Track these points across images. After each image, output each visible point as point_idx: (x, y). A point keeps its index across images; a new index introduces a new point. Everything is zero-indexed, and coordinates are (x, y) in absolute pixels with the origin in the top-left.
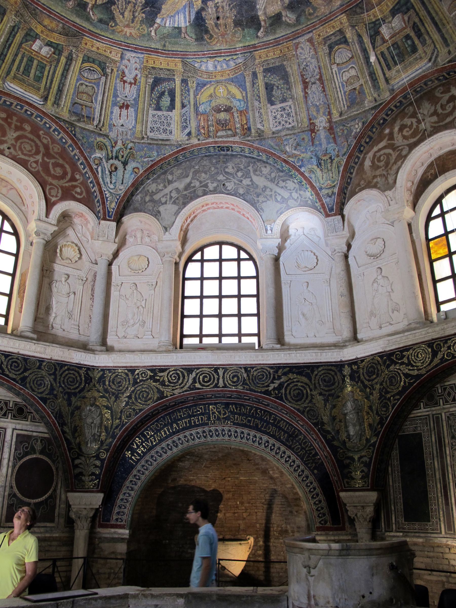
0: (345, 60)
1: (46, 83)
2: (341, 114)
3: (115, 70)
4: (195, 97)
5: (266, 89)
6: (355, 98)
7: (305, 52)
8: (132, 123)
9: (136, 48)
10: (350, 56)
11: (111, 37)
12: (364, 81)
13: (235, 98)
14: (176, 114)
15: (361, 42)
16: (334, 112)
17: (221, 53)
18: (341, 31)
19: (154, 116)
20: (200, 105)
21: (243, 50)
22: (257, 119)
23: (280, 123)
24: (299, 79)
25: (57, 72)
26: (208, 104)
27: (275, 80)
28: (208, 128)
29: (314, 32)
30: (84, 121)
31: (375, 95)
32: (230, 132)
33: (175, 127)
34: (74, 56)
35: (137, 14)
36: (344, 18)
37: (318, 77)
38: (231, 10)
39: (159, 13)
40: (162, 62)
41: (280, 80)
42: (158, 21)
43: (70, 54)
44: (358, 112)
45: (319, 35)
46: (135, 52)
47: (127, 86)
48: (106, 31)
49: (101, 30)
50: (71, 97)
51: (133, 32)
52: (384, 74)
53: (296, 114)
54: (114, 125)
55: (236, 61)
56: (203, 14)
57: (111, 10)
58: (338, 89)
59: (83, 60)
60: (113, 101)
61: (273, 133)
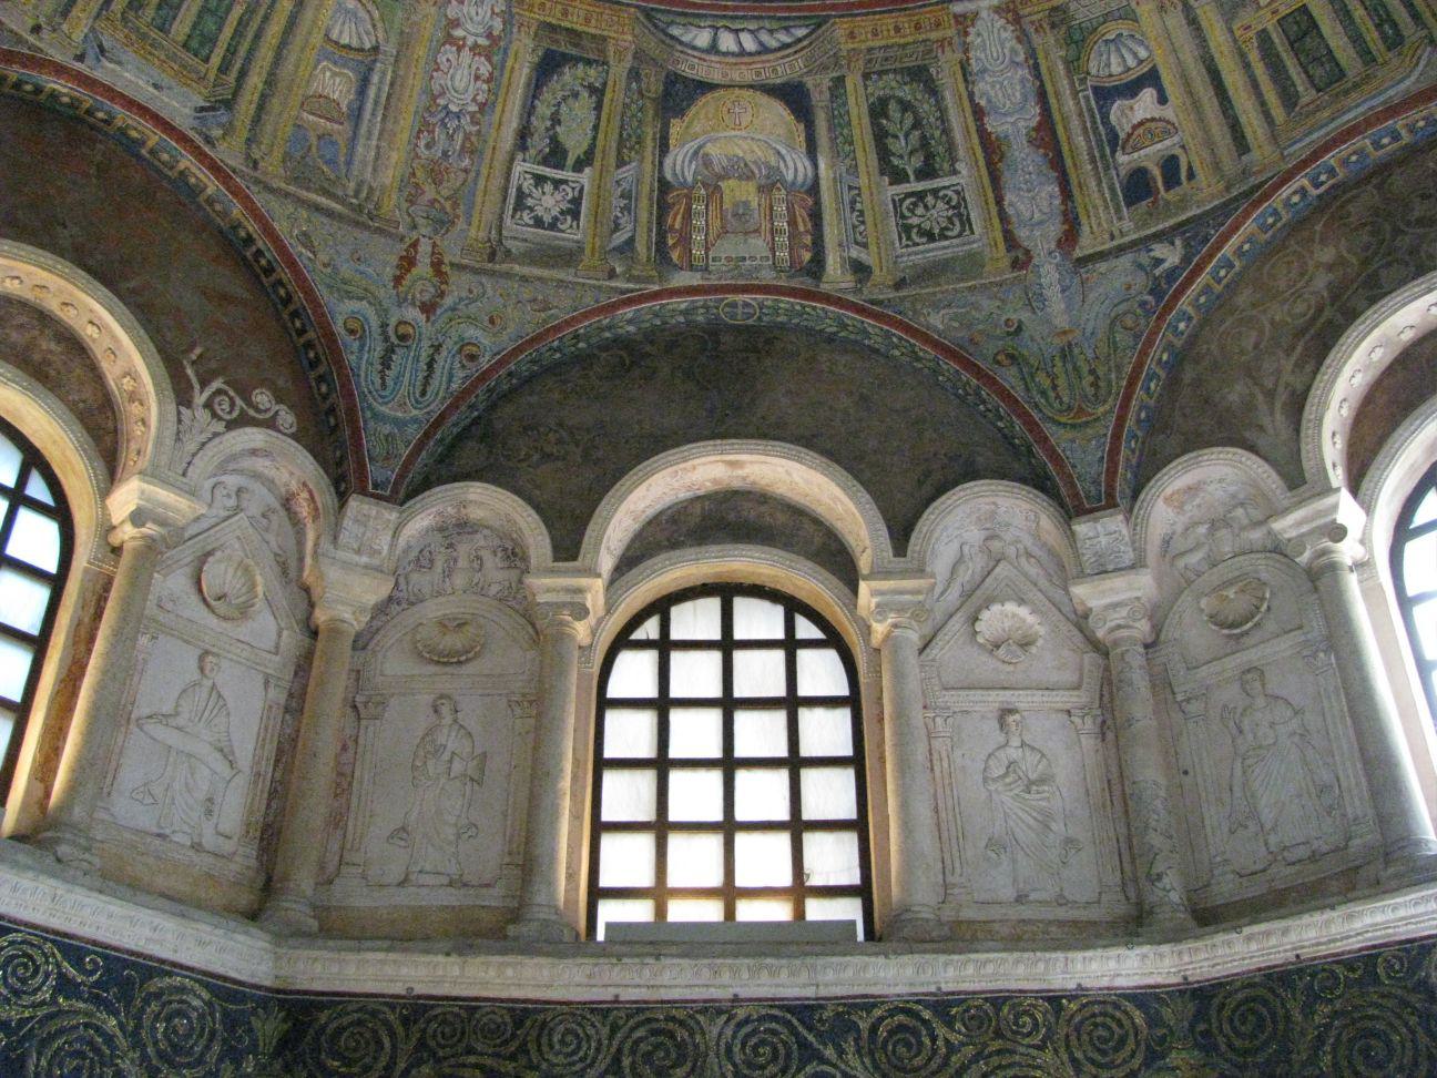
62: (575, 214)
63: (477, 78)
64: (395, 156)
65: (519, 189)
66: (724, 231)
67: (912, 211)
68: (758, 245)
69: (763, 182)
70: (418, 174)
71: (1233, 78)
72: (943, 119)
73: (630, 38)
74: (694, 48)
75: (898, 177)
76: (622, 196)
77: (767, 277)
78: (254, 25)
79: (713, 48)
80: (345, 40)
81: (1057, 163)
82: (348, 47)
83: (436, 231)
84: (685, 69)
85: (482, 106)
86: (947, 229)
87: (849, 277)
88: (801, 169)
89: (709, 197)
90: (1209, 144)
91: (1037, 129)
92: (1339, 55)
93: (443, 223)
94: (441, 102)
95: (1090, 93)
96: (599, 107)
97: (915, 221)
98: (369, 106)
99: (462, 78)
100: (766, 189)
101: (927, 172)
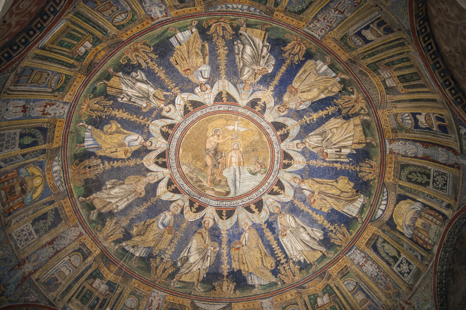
0: (73, 264)
1: (56, 49)
2: (37, 280)
3: (56, 99)
4: (31, 163)
5: (43, 215)
6: (52, 283)
7: (73, 233)
8: (9, 117)
9: (71, 112)
10: (77, 266)
11: (82, 95)
12: (65, 284)
13: (34, 193)
14: (17, 151)
15: (87, 270)
16: (38, 273)
17: (66, 174)
18: (91, 252)
19: (15, 134)
20: (25, 168)
21: (69, 189)
22: (19, 217)
23: (19, 236)
24: (54, 236)
25: (63, 57)
26: (27, 174)
27: (50, 219)
28: (7, 181)
29: (87, 235)
30: (15, 78)
31: (58, 298)
32: (5, 200)
33: (6, 153)
34: (73, 69)
35: (96, 112)
36: (98, 252)
37: (58, 249)
38: (95, 175)
39: (95, 128)
40: (59, 132)
41: (51, 222)
42: (90, 127)
43: (75, 67)
44: (43, 292)
45: (85, 239)
46: (68, 112)
47: (42, 109)
48: (87, 92)
49: (89, 89)
50: (40, 67)
51: (84, 111)
52: (73, 296)
53: (28, 246)
54: (7, 103)
55: (61, 186)
56: (93, 157)
57: (101, 95)
58: (54, 268)
59: (68, 75)
60: (30, 99)
61: (10, 235)
62: (410, 264)
63: (372, 265)
64: (380, 294)
65: (399, 271)
66: (427, 232)
67: (437, 185)
68: (433, 226)
69: (419, 216)
70: (386, 291)
71: (416, 96)
72: (416, 166)
73: (375, 228)
74: (382, 215)
75: (427, 184)
76: (410, 250)
77: (443, 230)
78: (341, 305)
79: (384, 211)
80: (352, 288)
81: (434, 144)
82: (354, 289)
83: (400, 297)
84: (386, 219)
85: (378, 268)
86: (444, 179)
87: (450, 210)
88: (419, 205)
89: (418, 231)
90: (433, 108)
91: (423, 146)
92: (410, 72)
93: (398, 295)
94: (373, 276)
95: (415, 130)
96: (388, 243)
97: (440, 186)
98: (367, 292)
99: (370, 268)
100: (421, 217)
101: (428, 176)
